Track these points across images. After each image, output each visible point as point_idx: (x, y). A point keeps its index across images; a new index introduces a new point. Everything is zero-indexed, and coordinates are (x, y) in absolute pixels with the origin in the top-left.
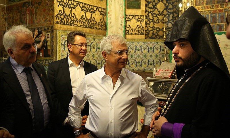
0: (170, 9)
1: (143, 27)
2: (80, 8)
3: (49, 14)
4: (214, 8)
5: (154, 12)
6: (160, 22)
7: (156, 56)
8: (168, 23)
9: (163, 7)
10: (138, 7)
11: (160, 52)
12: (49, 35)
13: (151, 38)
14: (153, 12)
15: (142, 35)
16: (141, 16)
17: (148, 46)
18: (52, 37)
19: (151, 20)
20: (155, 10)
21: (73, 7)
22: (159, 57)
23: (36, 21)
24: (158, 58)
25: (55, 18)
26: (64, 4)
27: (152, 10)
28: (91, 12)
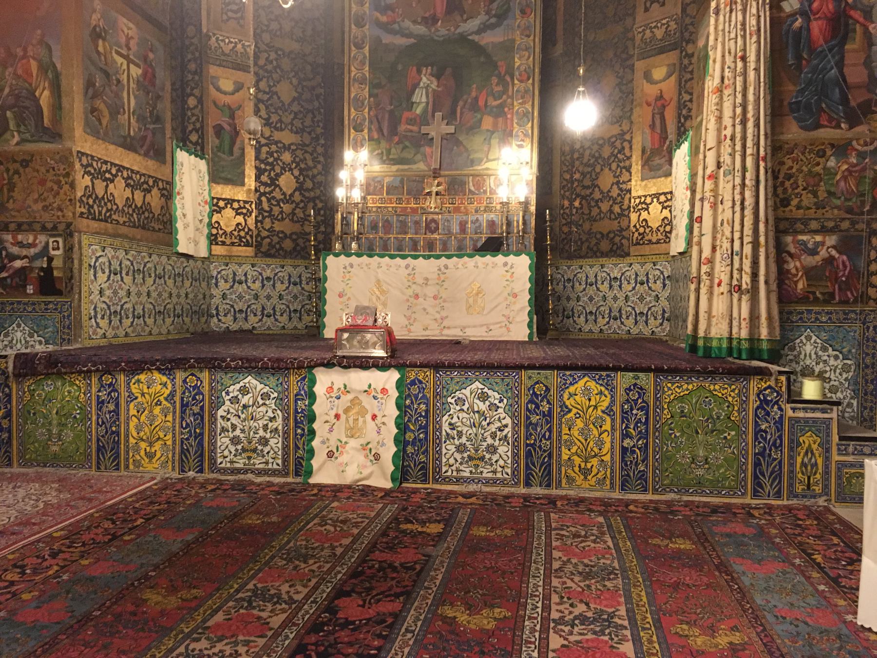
1: (249, 230)
2: (123, 181)
3: (58, 193)
7: (281, 297)
9: (294, 185)
10: (239, 181)
11: (287, 288)
12: (57, 242)
13: (267, 255)
14: (271, 192)
15: (248, 248)
16: (245, 202)
17: (261, 274)
18: (69, 250)
20: (274, 190)
21: (109, 179)
22: (287, 300)
23: (10, 205)
24: (284, 302)
25: (78, 204)
26: (93, 171)
27: (268, 189)
28: (144, 190)
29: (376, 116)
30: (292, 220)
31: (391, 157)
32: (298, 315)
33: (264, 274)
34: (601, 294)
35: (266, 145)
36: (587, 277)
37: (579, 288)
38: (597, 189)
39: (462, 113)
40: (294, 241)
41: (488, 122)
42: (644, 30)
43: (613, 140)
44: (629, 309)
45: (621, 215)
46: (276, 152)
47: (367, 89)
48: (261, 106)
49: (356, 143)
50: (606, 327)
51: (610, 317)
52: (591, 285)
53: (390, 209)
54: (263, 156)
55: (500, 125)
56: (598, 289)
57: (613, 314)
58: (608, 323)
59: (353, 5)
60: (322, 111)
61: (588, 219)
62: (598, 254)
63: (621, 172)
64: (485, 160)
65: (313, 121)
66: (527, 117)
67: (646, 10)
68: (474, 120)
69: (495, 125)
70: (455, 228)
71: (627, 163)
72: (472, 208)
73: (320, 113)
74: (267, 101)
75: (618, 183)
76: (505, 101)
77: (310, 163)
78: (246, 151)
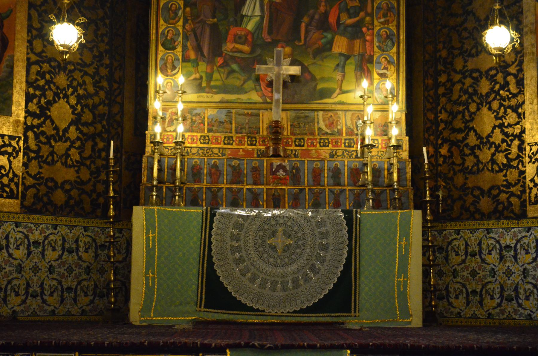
0: (86, 124)
1: (15, 175)
4: (232, 144)
5: (41, 129)
6: (58, 161)
7: (51, 270)
8: (79, 167)
9: (70, 117)
11: (60, 257)
14: (39, 126)
15: (12, 201)
16: (11, 138)
17: (27, 237)
19: (33, 152)
20: (44, 122)
24: (55, 276)
27: (36, 122)
29: (194, 31)
30: (65, 164)
31: (212, 83)
32: (72, 295)
33: (32, 238)
34: (488, 268)
35: (37, 63)
36: (467, 244)
37: (455, 259)
38: (472, 133)
39: (307, 32)
40: (67, 192)
41: (340, 45)
43: (493, 72)
44: (529, 286)
45: (508, 166)
46: (49, 72)
49: (165, 65)
50: (497, 310)
51: (502, 296)
52: (473, 255)
53: (215, 151)
54: (33, 77)
55: (356, 48)
56: (483, 261)
57: (505, 294)
58: (499, 305)
60: (107, 21)
61: (460, 171)
62: (477, 216)
63: (505, 112)
64: (338, 91)
65: (96, 35)
66: (392, 40)
68: (323, 41)
69: (351, 48)
70: (306, 178)
71: (513, 102)
72: (325, 152)
73: (105, 24)
74: (40, 6)
76: (362, 21)
78: (16, 70)
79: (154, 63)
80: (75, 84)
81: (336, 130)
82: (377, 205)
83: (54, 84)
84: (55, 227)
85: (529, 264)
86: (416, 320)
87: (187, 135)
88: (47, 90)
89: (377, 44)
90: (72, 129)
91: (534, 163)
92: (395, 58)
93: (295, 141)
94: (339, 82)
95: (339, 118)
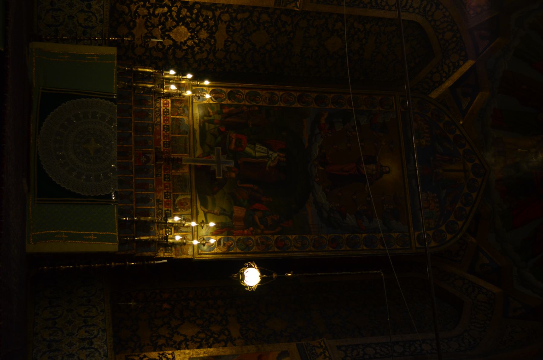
4: (164, 130)
6: (148, 30)
14: (171, 16)
19: (154, 12)
20: (174, 20)
27: (174, 14)
31: (207, 124)
41: (239, 212)
42: (322, 347)
43: (226, 332)
46: (208, 25)
47: (264, 104)
48: (247, 15)
53: (158, 120)
59: (332, 95)
63: (197, 342)
64: (206, 210)
67: (339, 348)
72: (161, 196)
75: (186, 340)
77: (198, 57)
79: (218, 85)
80: (202, 45)
81: (177, 207)
82: (122, 224)
83: (200, 29)
84: (101, 21)
85: (78, 358)
86: (31, 248)
87: (169, 100)
88: (196, 23)
89: (241, 238)
90: (171, 42)
91: (159, 356)
92: (232, 251)
93: (168, 175)
94: (212, 212)
95: (187, 210)
